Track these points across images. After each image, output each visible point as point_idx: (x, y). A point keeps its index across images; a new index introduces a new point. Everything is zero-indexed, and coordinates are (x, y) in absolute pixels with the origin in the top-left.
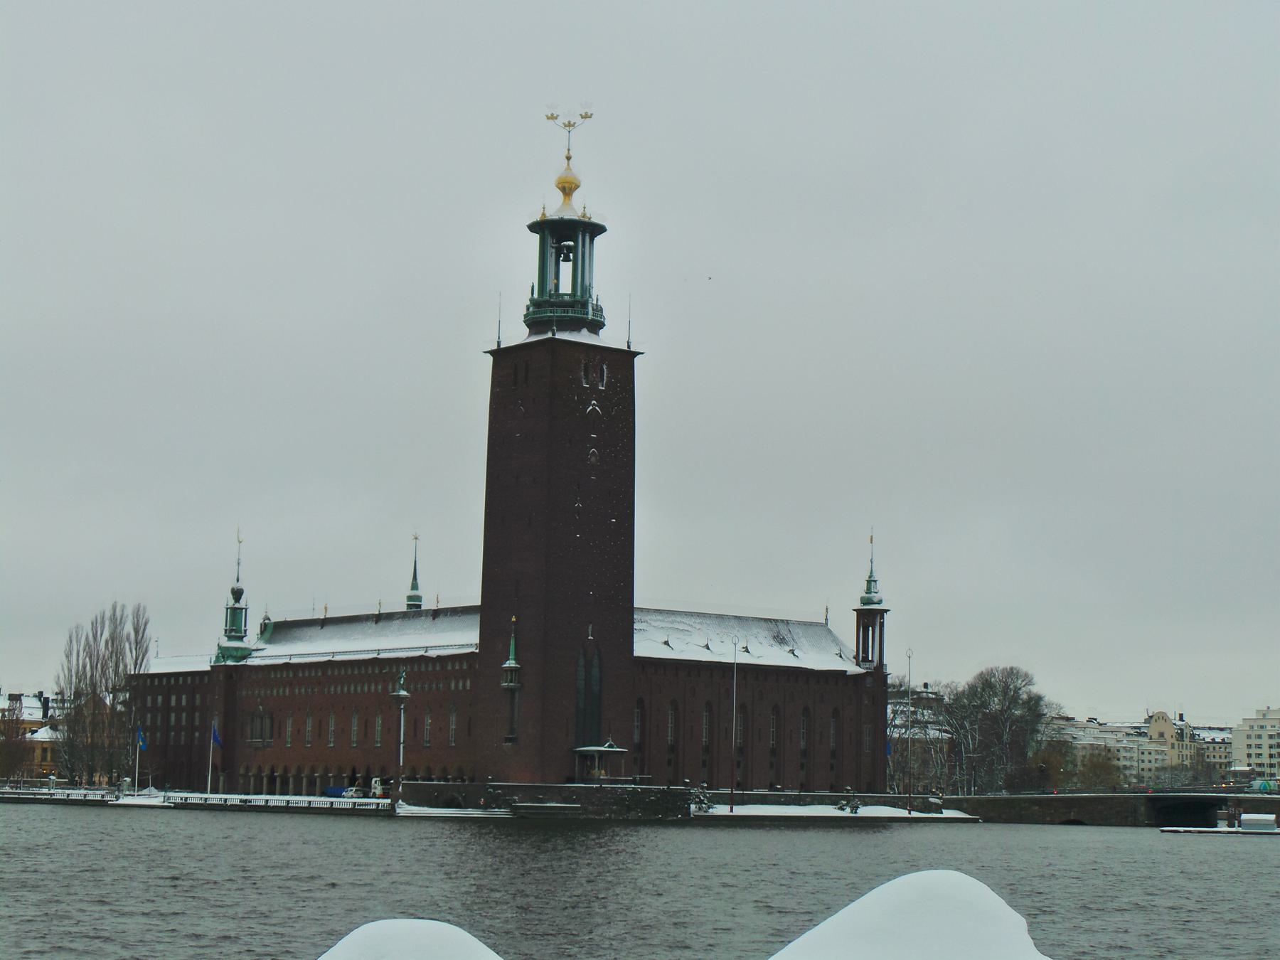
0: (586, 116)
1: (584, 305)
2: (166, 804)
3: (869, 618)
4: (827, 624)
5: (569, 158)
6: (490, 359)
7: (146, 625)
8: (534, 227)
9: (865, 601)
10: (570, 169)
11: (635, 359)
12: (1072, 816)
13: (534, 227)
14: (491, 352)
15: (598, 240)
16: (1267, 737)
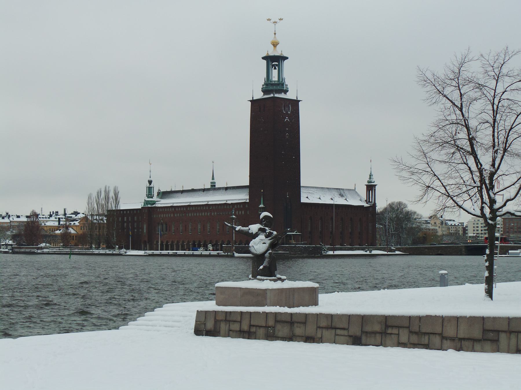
0: (281, 19)
1: (283, 84)
2: (145, 254)
3: (371, 188)
4: (355, 190)
5: (275, 34)
6: (251, 103)
7: (118, 193)
8: (263, 58)
9: (369, 182)
10: (276, 38)
11: (299, 103)
12: (439, 252)
13: (263, 58)
14: (250, 101)
15: (286, 61)
16: (480, 224)
